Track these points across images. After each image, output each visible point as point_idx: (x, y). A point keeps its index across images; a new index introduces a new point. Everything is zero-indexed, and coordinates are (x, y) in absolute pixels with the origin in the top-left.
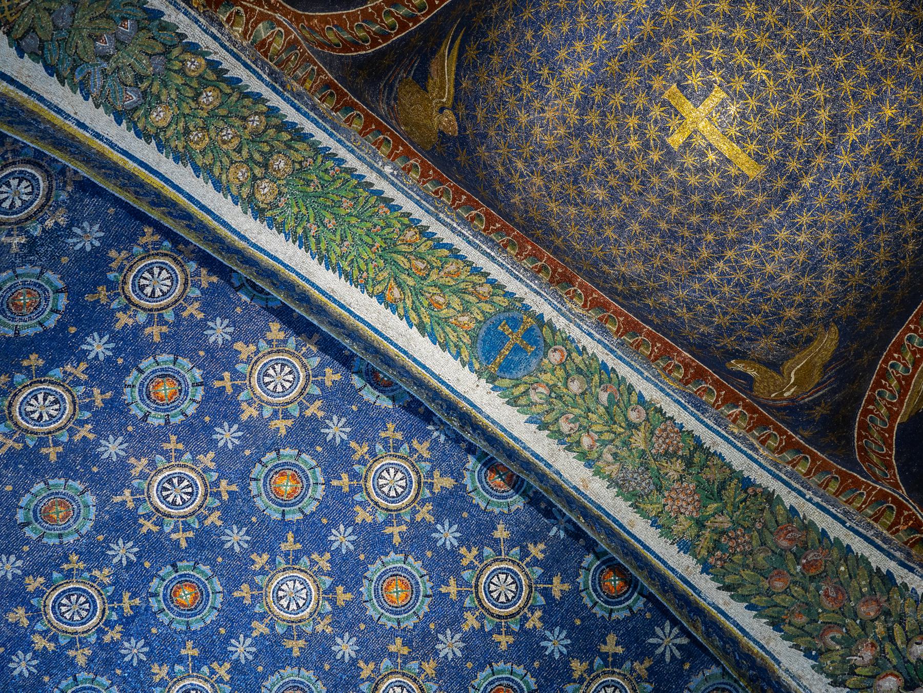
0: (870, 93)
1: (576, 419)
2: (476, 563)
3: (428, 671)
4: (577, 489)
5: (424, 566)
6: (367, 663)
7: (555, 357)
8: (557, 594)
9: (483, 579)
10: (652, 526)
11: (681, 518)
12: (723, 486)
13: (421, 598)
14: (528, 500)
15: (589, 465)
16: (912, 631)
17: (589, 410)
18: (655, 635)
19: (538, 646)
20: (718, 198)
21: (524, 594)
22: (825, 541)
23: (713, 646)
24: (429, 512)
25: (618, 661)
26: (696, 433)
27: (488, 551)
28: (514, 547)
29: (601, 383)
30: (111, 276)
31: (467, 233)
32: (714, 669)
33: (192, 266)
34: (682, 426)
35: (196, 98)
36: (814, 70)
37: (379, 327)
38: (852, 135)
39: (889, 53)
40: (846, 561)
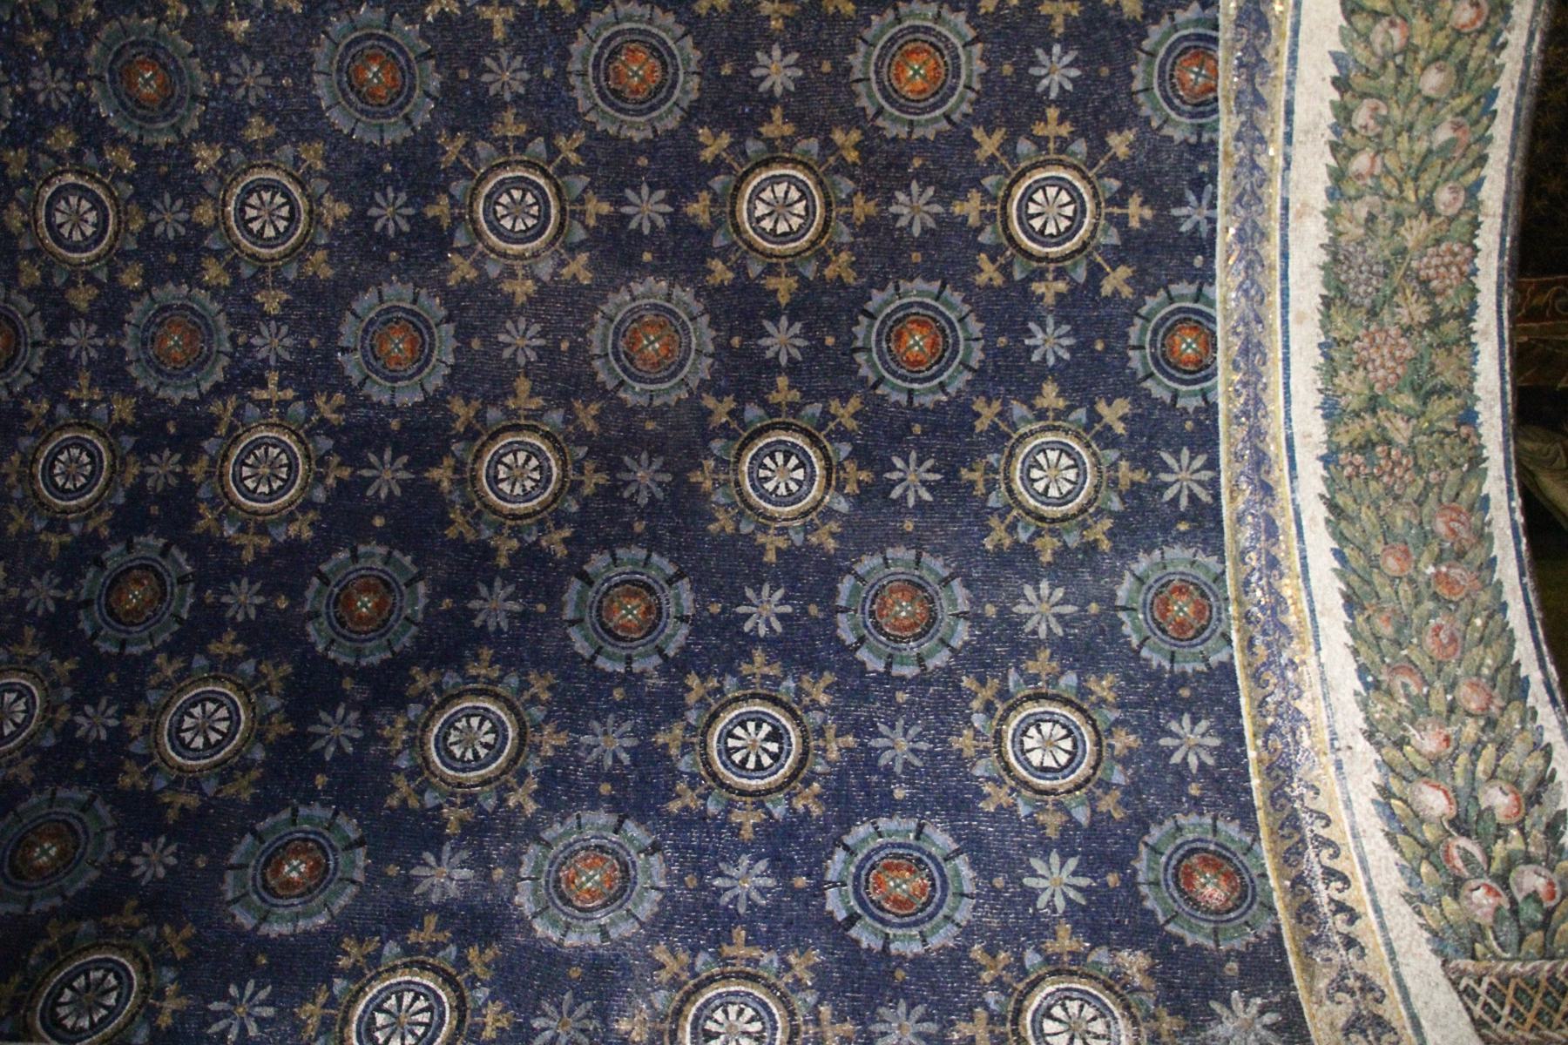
1: (1384, 122)
2: (1051, 145)
3: (857, 211)
4: (1285, 207)
5: (984, 78)
6: (786, 116)
8: (1107, 289)
9: (1039, 175)
10: (1320, 345)
11: (1360, 373)
12: (1444, 390)
13: (938, 113)
15: (1330, 195)
16: (1506, 772)
17: (1410, 128)
18: (1176, 454)
19: (1025, 323)
21: (1068, 246)
22: (1485, 573)
23: (1234, 535)
24: (1067, 15)
25: (1107, 438)
26: (1479, 299)
27: (1080, 147)
28: (1116, 177)
34: (1475, 272)
40: (1490, 617)
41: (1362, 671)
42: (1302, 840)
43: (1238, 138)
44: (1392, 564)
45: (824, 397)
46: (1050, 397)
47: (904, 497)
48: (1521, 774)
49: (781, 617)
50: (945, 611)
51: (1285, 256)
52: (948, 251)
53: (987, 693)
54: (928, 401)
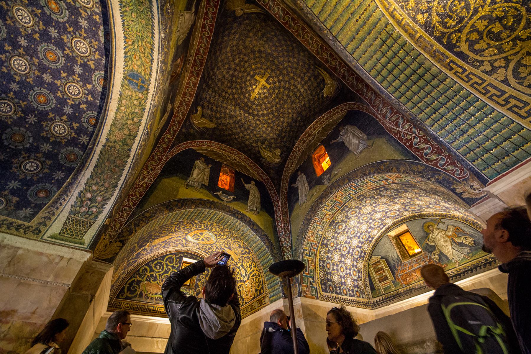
0: (270, 121)
7: (140, 95)
8: (81, 106)
12: (127, 145)
20: (244, 91)
21: (76, 97)
25: (72, 128)
31: (160, 64)
32: (82, 153)
36: (274, 109)
37: (117, 38)
38: (261, 119)
39: (277, 124)
45: (20, 99)
46: (65, 118)
52: (52, 88)
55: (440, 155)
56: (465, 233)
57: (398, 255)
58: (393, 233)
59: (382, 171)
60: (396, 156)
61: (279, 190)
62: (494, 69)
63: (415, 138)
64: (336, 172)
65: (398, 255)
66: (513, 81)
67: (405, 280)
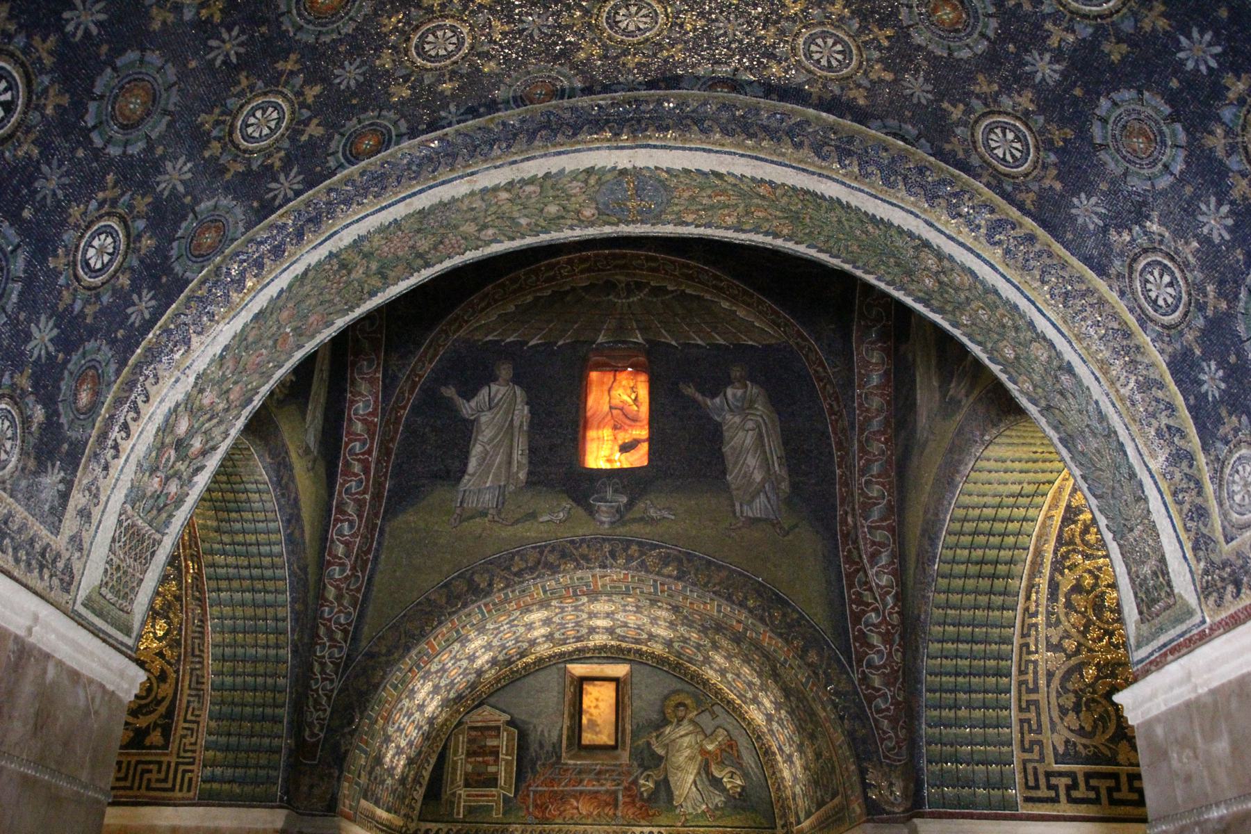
4: (472, 174)
12: (384, 277)
14: (499, 100)
15: (481, 191)
18: (299, 173)
29: (537, 225)
30: (1053, 158)
33: (975, 161)
35: (1017, 358)
37: (759, 163)
41: (226, 348)
42: (128, 398)
43: (504, 124)
44: (285, 314)
46: (312, 92)
47: (212, 49)
48: (212, 439)
49: (87, 32)
50: (145, 128)
51: (443, 183)
53: (109, 194)
54: (287, 26)
55: (887, 685)
56: (738, 764)
57: (560, 736)
58: (578, 669)
59: (772, 622)
60: (818, 615)
61: (395, 378)
62: (1057, 648)
63: (876, 610)
64: (652, 512)
65: (560, 736)
66: (1056, 683)
67: (543, 808)
